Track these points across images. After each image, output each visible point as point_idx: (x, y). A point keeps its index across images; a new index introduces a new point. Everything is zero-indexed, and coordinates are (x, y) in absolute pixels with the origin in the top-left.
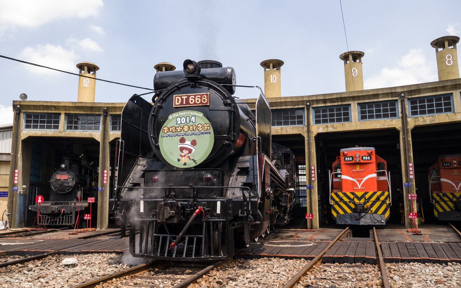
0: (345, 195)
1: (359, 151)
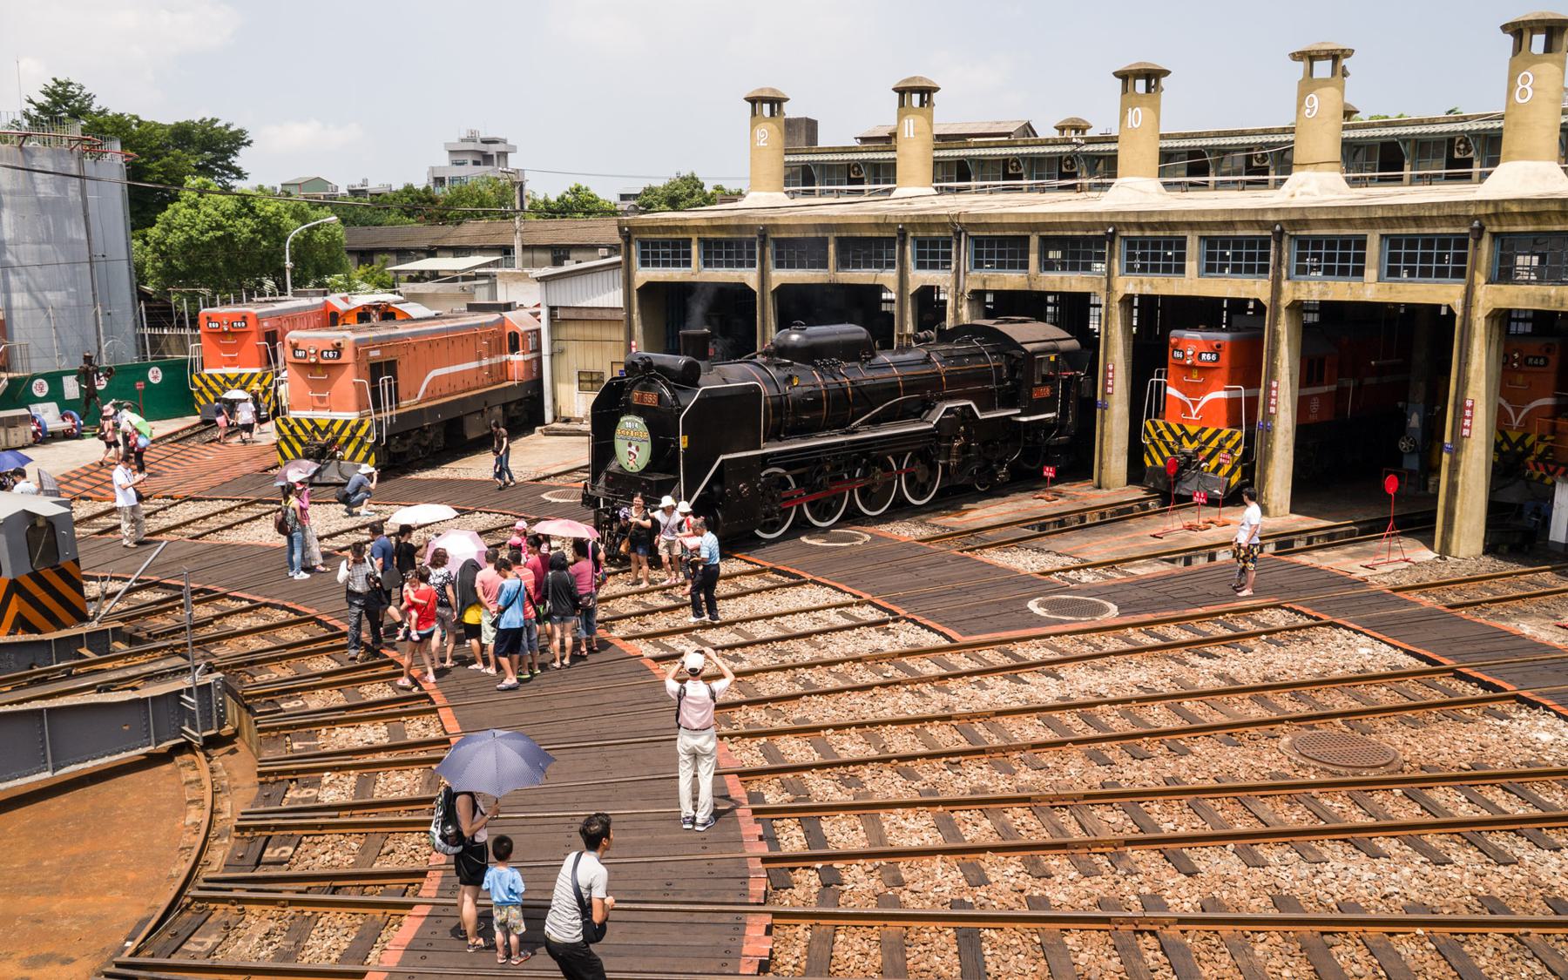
0: (1168, 427)
1: (1193, 341)
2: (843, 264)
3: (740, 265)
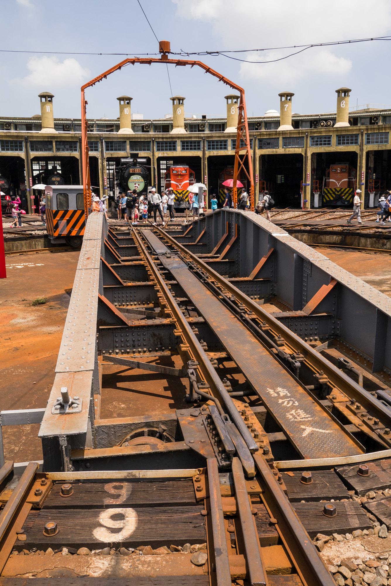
2: (58, 150)
3: (16, 150)
